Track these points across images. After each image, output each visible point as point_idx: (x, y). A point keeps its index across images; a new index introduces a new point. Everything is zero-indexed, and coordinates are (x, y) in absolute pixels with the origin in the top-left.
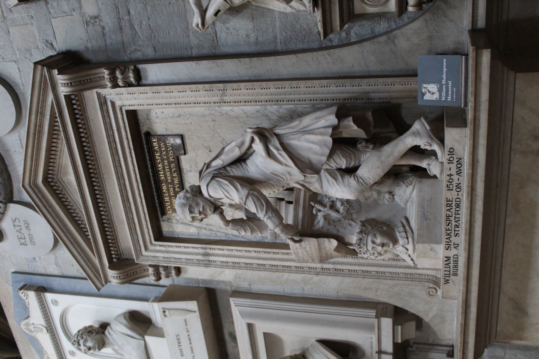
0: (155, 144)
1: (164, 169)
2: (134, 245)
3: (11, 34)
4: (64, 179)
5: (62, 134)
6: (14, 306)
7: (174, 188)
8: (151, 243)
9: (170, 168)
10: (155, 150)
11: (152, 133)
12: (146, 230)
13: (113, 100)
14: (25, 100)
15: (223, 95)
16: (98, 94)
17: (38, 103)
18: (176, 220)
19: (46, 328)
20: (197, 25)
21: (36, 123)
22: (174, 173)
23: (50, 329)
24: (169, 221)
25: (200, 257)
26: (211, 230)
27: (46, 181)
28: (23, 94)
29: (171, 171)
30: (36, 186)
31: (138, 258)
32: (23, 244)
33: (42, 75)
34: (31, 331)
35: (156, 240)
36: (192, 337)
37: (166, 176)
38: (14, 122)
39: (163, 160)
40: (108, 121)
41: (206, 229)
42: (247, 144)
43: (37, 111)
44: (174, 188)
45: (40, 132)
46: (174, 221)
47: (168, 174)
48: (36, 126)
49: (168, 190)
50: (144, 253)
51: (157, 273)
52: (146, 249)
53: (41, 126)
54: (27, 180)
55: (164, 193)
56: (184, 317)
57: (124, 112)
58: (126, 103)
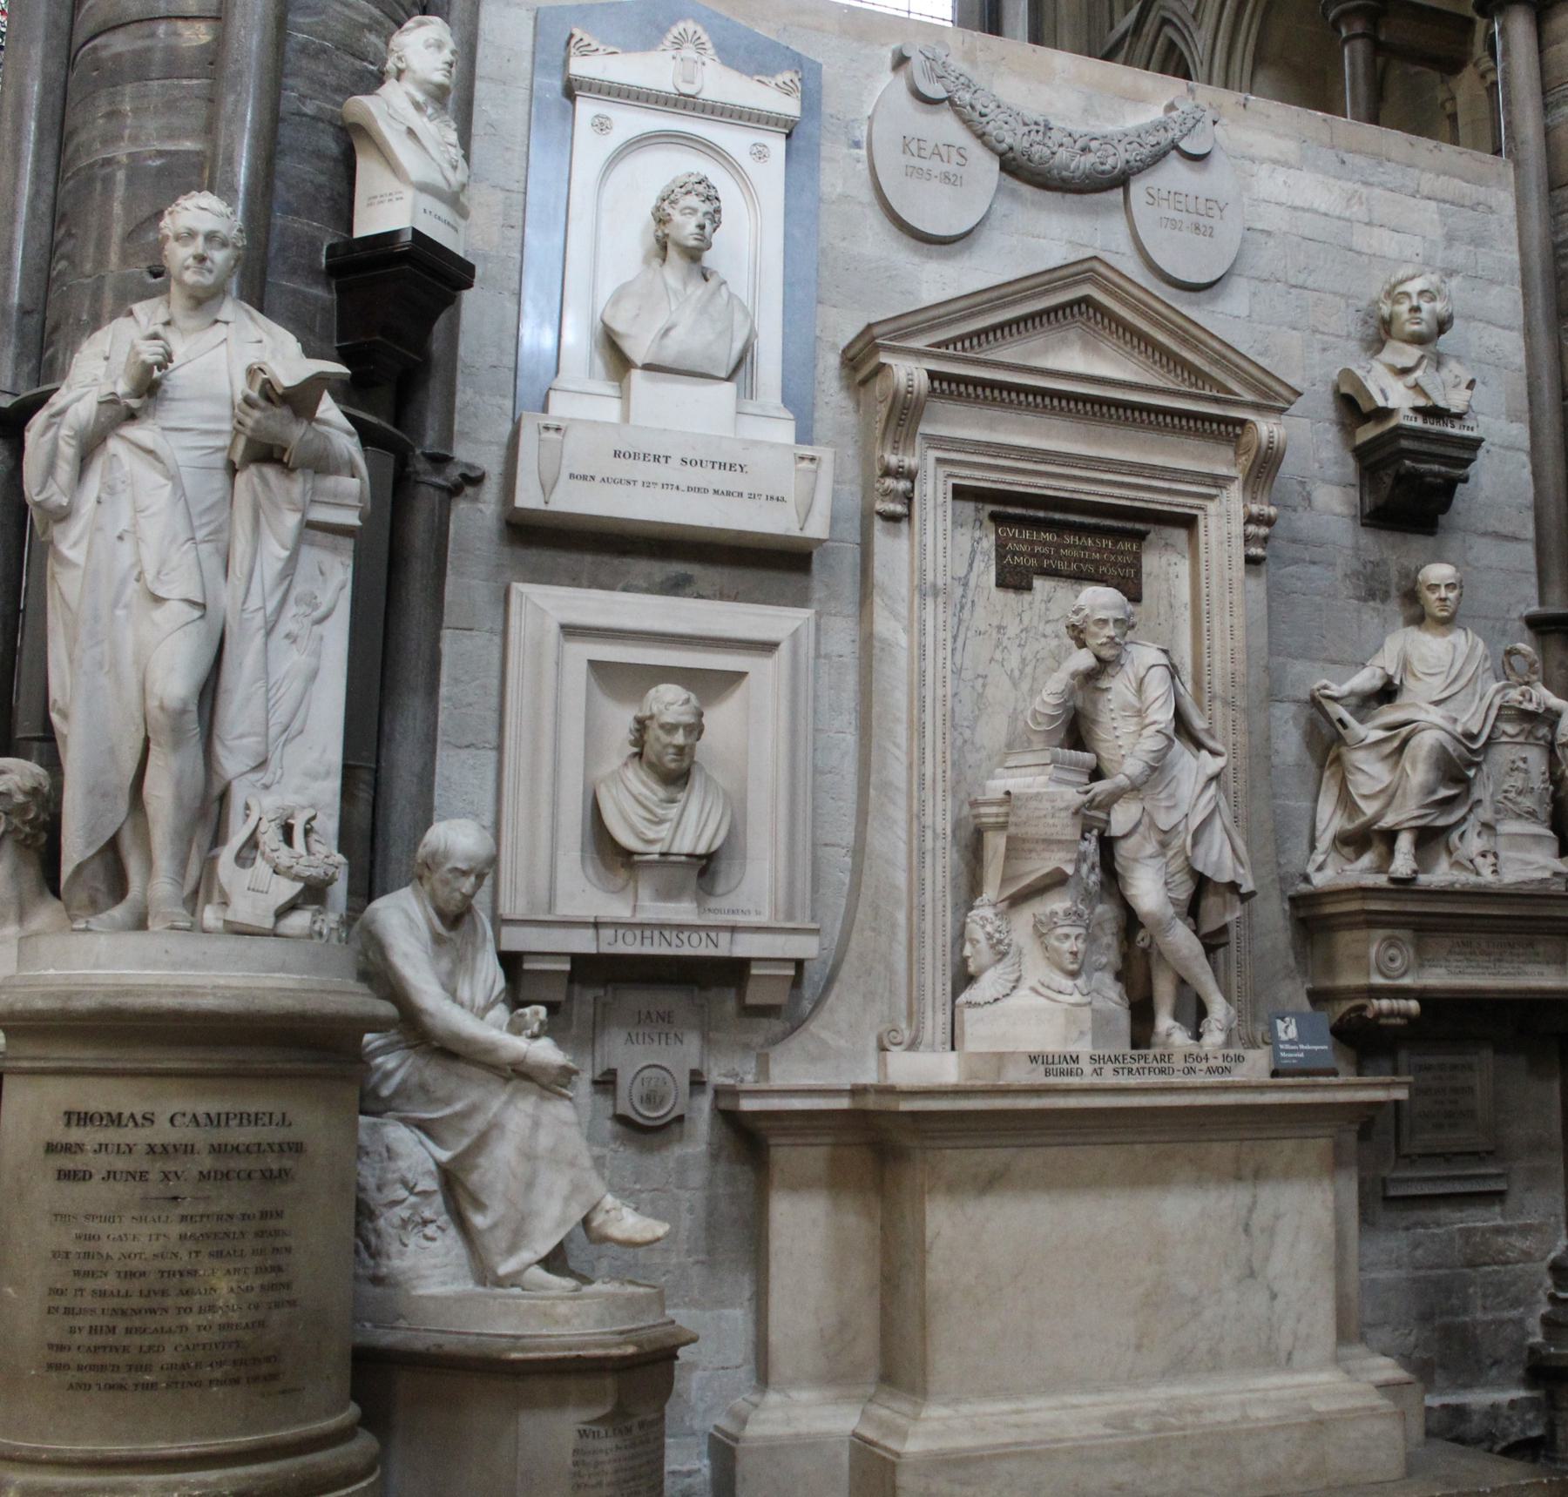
0: (1128, 545)
1: (1085, 548)
2: (953, 440)
3: (1290, 331)
4: (1072, 334)
5: (1184, 388)
6: (728, 20)
7: (1048, 557)
8: (950, 476)
9: (1085, 561)
10: (1117, 542)
11: (1144, 544)
12: (978, 474)
13: (1217, 500)
14: (1191, 304)
15: (1225, 703)
16: (1231, 479)
17: (1237, 366)
18: (980, 539)
19: (693, 97)
20: (1325, 687)
21: (1206, 345)
22: (1078, 567)
23: (684, 103)
24: (978, 524)
25: (930, 577)
26: (962, 607)
27: (1086, 300)
28: (1198, 304)
29: (1081, 560)
30: (1083, 281)
31: (926, 437)
32: (906, 145)
33: (1281, 396)
34: (678, 44)
35: (955, 486)
36: (735, 500)
37: (1068, 546)
38: (1159, 263)
39: (1099, 550)
40: (1188, 478)
41: (963, 596)
42: (1211, 743)
43: (1224, 357)
44: (1048, 557)
45: (1184, 341)
46: (978, 534)
47: (1075, 554)
48: (1201, 342)
49: (1045, 543)
50: (933, 454)
51: (902, 473)
52: (939, 461)
53: (1195, 349)
54: (1102, 269)
55: (1038, 533)
56: (791, 497)
57: (1194, 512)
58: (1212, 523)
